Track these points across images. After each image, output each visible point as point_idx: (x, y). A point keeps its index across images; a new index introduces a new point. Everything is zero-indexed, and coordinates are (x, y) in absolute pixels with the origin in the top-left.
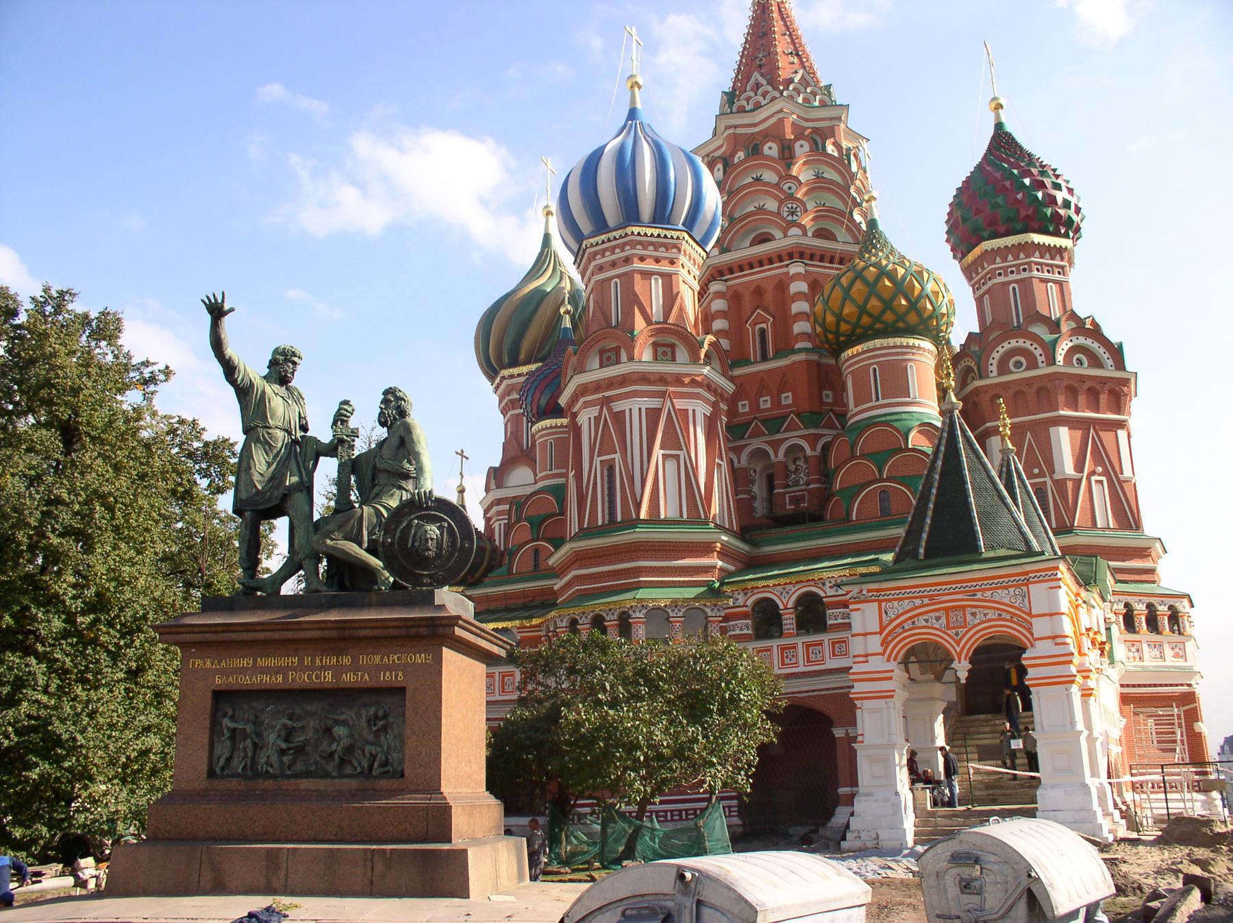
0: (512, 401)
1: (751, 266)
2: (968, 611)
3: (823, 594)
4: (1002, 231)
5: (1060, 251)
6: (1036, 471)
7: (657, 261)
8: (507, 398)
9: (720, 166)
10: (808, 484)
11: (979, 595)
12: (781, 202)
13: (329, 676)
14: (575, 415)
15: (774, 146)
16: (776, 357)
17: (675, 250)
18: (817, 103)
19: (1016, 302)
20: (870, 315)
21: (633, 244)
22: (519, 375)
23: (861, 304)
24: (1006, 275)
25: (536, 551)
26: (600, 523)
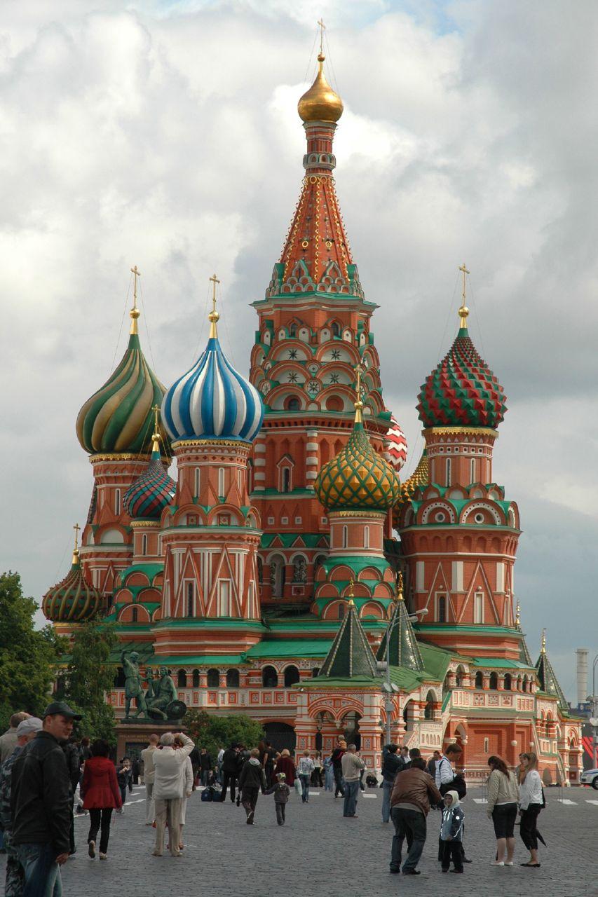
1: (283, 424)
5: (483, 437)
6: (441, 587)
7: (223, 459)
9: (268, 333)
10: (305, 582)
11: (346, 695)
12: (307, 381)
14: (170, 546)
15: (306, 330)
16: (292, 493)
17: (234, 452)
18: (341, 292)
19: (449, 469)
20: (344, 498)
22: (114, 460)
23: (340, 490)
24: (445, 452)
25: (135, 610)
26: (184, 616)
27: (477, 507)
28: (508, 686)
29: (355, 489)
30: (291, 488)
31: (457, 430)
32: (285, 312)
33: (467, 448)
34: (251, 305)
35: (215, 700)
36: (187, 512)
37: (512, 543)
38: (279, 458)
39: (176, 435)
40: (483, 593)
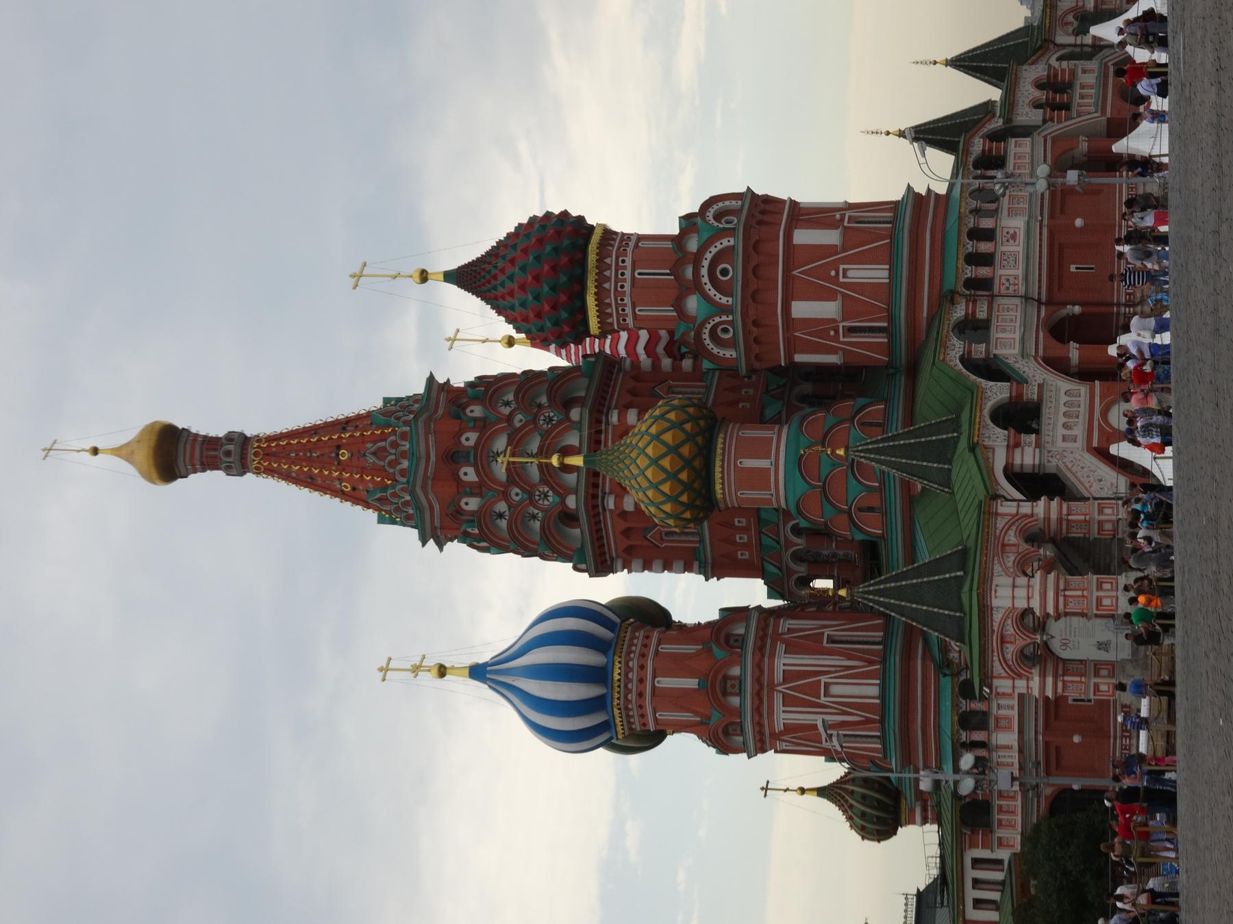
2: (1005, 633)
5: (600, 260)
6: (832, 333)
7: (641, 681)
11: (995, 628)
12: (532, 502)
15: (464, 500)
18: (408, 446)
21: (627, 700)
24: (627, 315)
27: (705, 279)
28: (989, 235)
29: (681, 488)
32: (441, 522)
33: (619, 284)
34: (441, 549)
35: (1009, 719)
36: (721, 736)
37: (763, 212)
40: (842, 267)
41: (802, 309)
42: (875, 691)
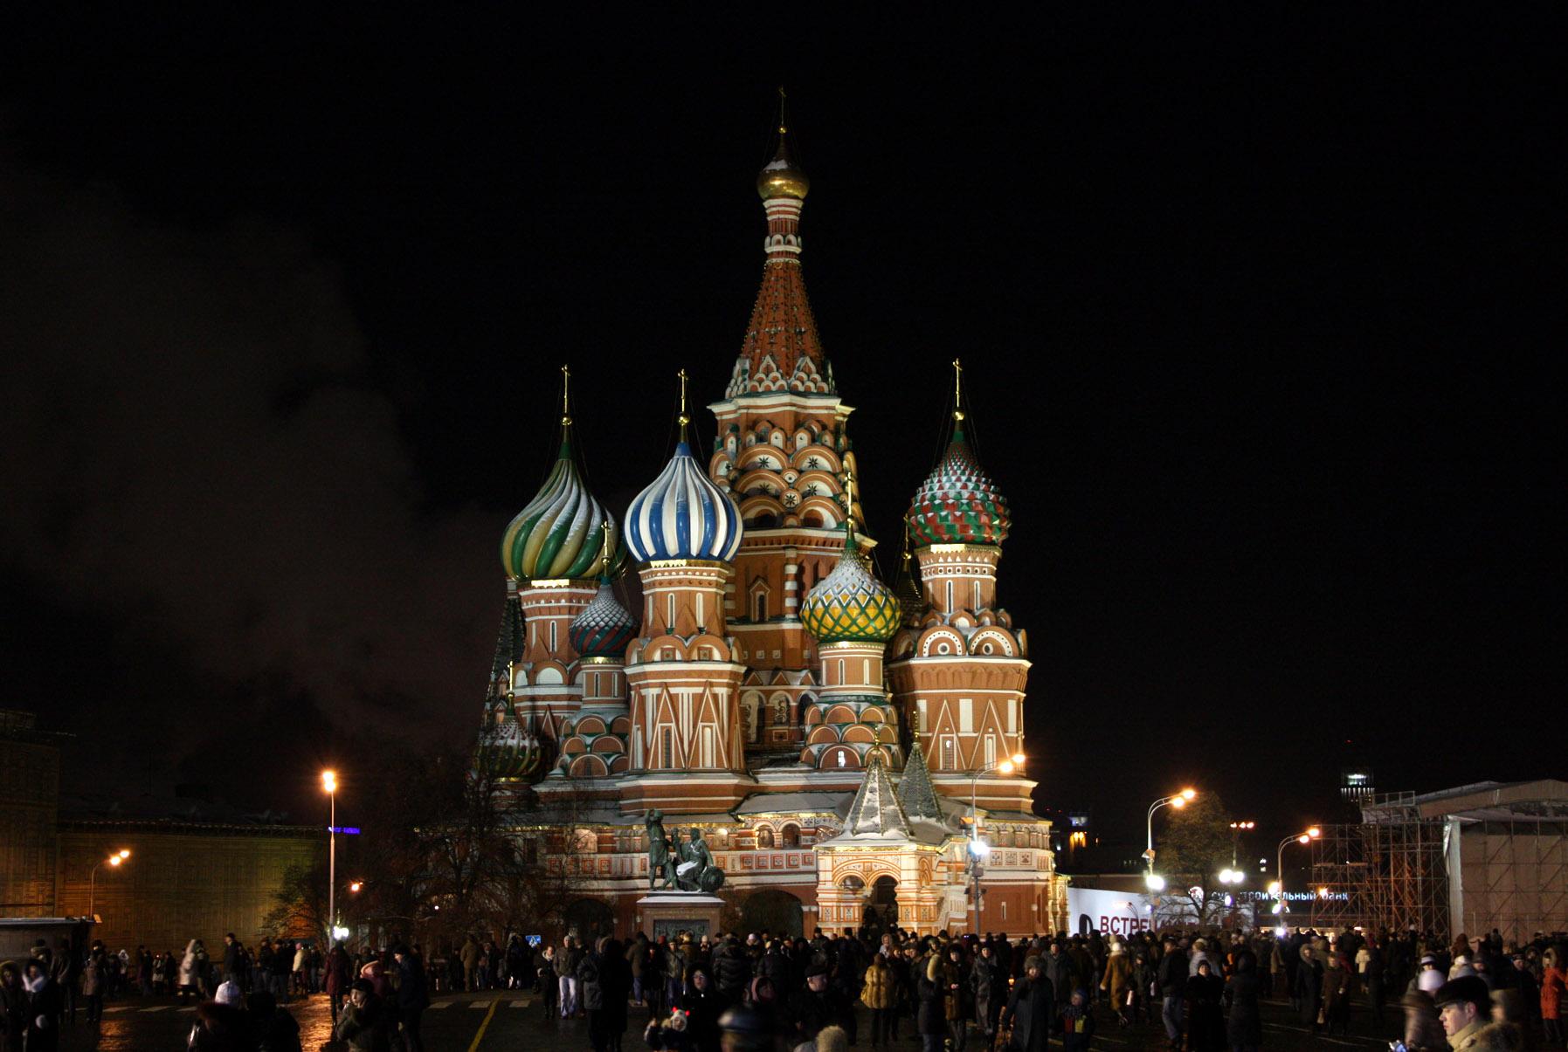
0: (539, 608)
3: (800, 826)
4: (946, 537)
6: (947, 729)
7: (700, 583)
8: (535, 605)
10: (790, 726)
11: (879, 858)
13: (688, 917)
14: (640, 687)
17: (713, 574)
18: (815, 391)
20: (841, 626)
22: (548, 588)
23: (836, 618)
24: (946, 573)
30: (767, 619)
31: (960, 547)
38: (752, 581)
39: (647, 559)
40: (994, 736)
41: (966, 707)
42: (708, 764)
